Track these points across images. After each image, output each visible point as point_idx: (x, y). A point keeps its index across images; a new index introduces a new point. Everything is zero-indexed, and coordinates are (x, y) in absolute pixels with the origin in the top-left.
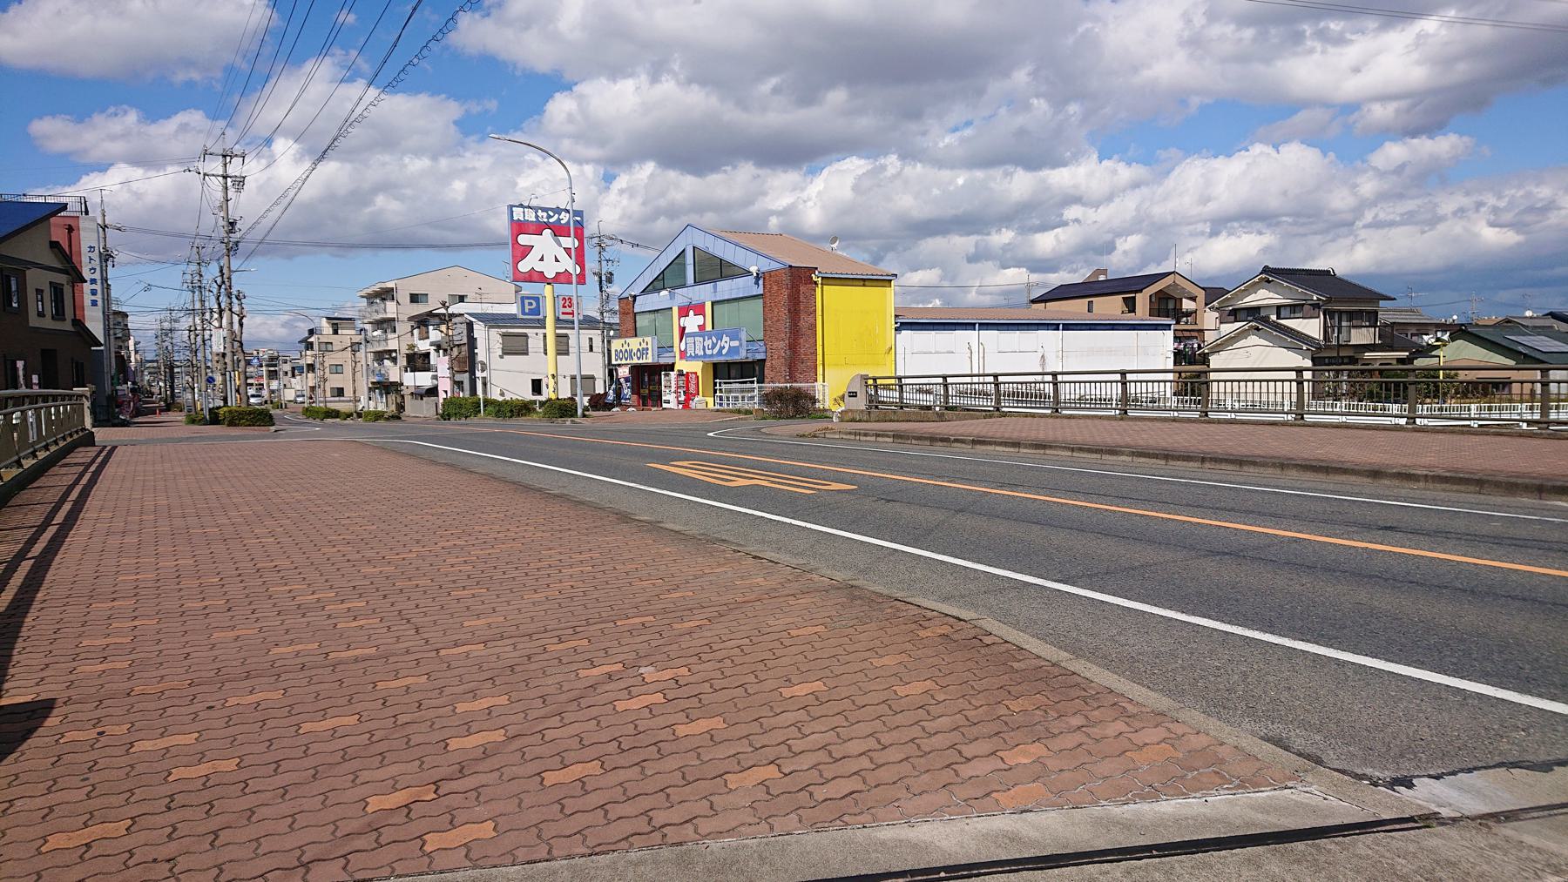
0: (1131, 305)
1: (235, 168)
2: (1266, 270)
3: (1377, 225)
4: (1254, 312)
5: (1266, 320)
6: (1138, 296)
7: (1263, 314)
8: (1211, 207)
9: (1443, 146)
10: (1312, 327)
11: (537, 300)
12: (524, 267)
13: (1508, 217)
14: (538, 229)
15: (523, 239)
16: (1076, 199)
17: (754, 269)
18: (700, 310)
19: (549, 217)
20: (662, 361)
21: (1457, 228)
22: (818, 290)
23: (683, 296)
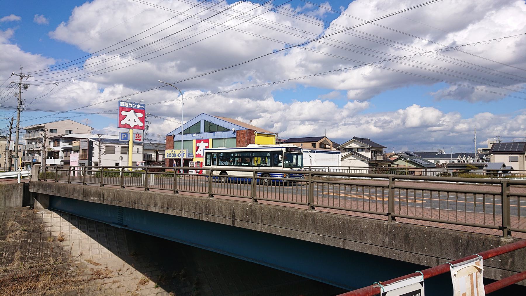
0: (314, 146)
1: (24, 80)
2: (354, 138)
3: (345, 125)
4: (350, 149)
5: (354, 152)
6: (317, 143)
7: (353, 150)
8: (302, 116)
9: (364, 104)
10: (368, 155)
11: (127, 134)
12: (123, 123)
13: (380, 124)
14: (129, 109)
15: (123, 113)
16: (265, 111)
17: (233, 129)
18: (206, 141)
19: (133, 106)
20: (189, 158)
21: (364, 126)
22: (256, 137)
23: (196, 136)
